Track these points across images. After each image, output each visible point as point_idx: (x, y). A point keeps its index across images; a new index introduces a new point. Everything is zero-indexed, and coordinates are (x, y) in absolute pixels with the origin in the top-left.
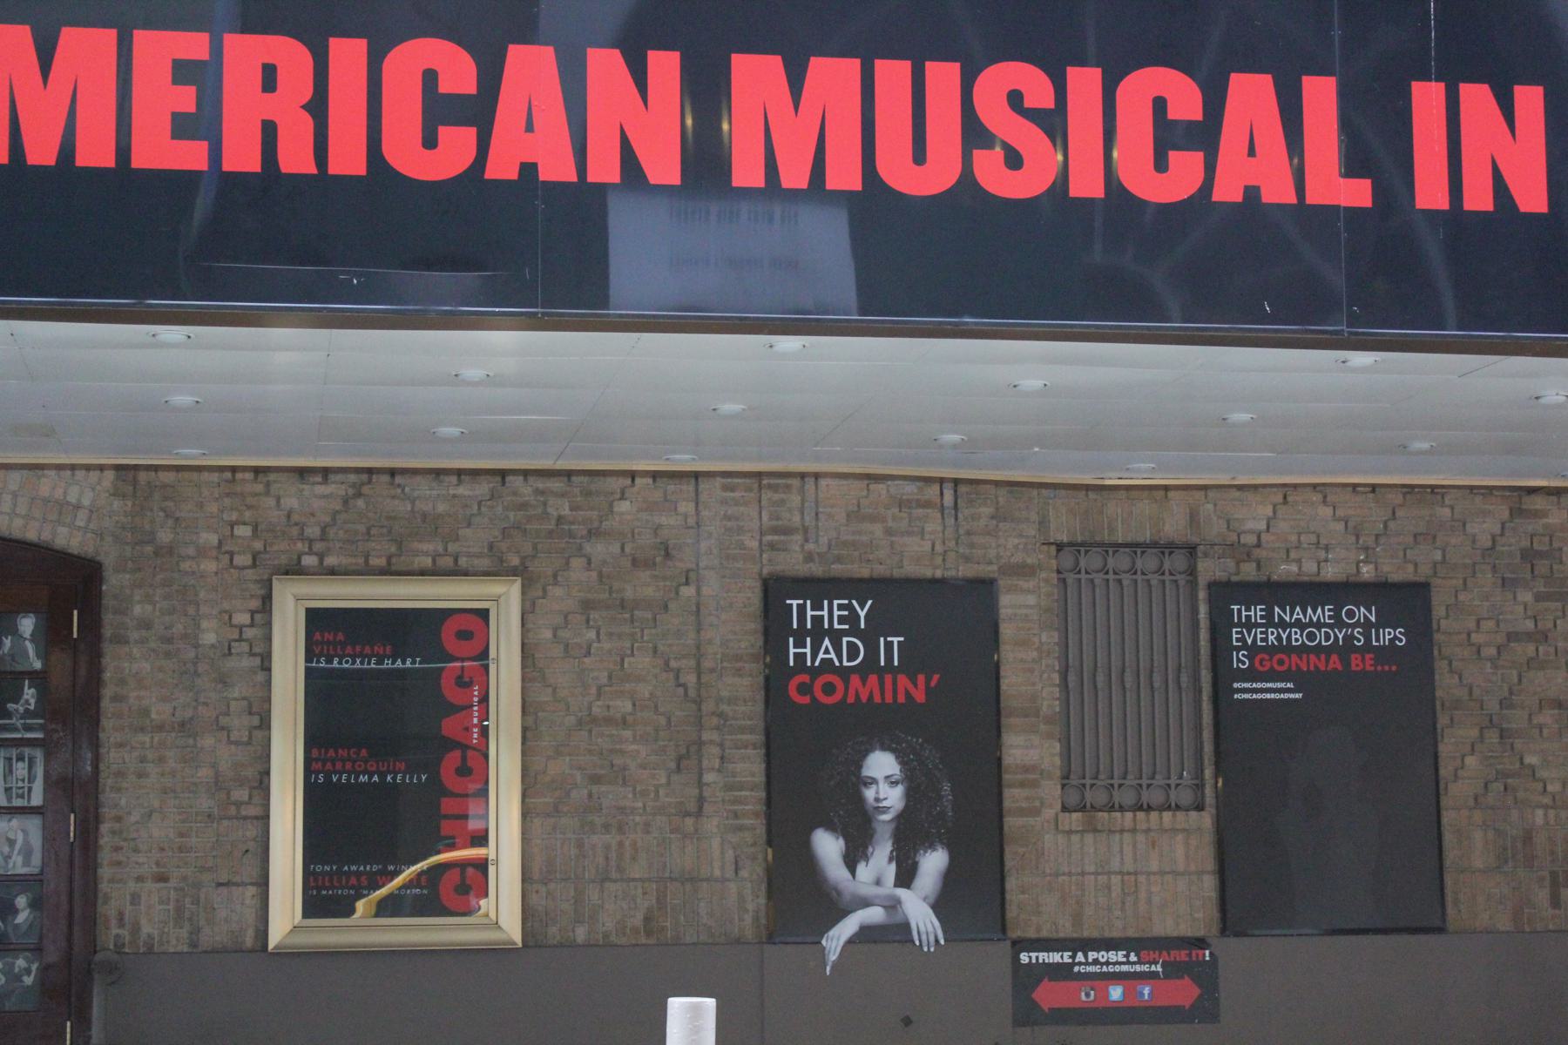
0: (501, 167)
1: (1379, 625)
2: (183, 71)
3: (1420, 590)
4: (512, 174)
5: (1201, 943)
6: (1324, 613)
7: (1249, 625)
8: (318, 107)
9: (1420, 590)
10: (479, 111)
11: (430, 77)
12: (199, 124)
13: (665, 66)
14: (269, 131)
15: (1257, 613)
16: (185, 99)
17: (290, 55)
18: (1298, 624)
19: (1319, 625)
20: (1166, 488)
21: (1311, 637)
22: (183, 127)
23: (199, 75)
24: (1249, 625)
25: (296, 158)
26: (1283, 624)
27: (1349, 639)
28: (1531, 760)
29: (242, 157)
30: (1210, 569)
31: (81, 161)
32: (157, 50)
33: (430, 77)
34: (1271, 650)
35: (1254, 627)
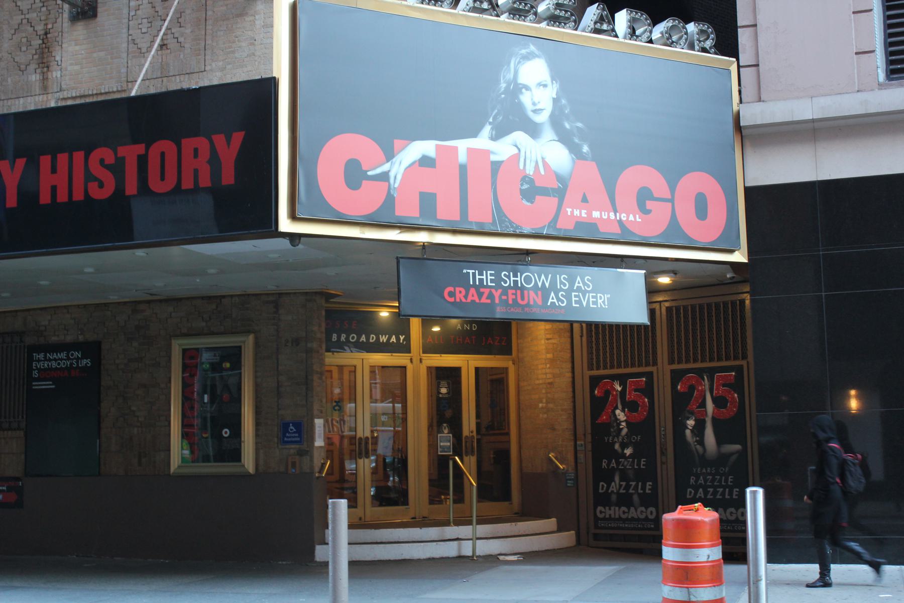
1: (82, 358)
3: (97, 345)
5: (17, 479)
6: (63, 355)
7: (39, 361)
9: (97, 345)
15: (41, 356)
18: (55, 360)
19: (61, 360)
20: (16, 311)
21: (59, 364)
24: (39, 361)
26: (50, 360)
27: (71, 364)
28: (134, 408)
30: (29, 340)
34: (45, 370)
35: (41, 362)
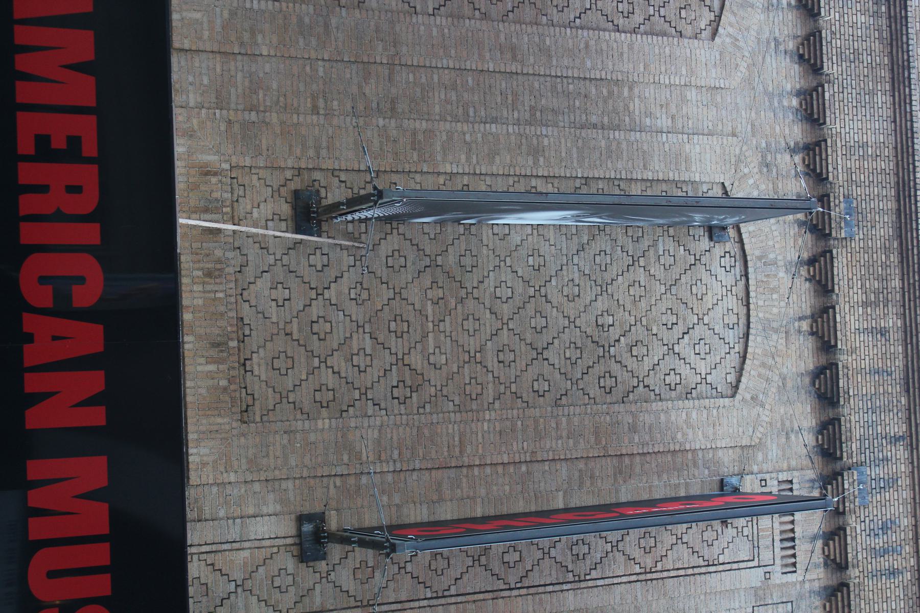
0: (30, 323)
2: (74, 142)
4: (26, 329)
8: (59, 216)
10: (63, 309)
11: (81, 280)
12: (45, 151)
13: (97, 417)
14: (42, 189)
16: (58, 143)
17: (88, 201)
22: (42, 141)
23: (72, 151)
25: (28, 204)
29: (28, 173)
31: (19, 84)
32: (86, 128)
33: (81, 280)
